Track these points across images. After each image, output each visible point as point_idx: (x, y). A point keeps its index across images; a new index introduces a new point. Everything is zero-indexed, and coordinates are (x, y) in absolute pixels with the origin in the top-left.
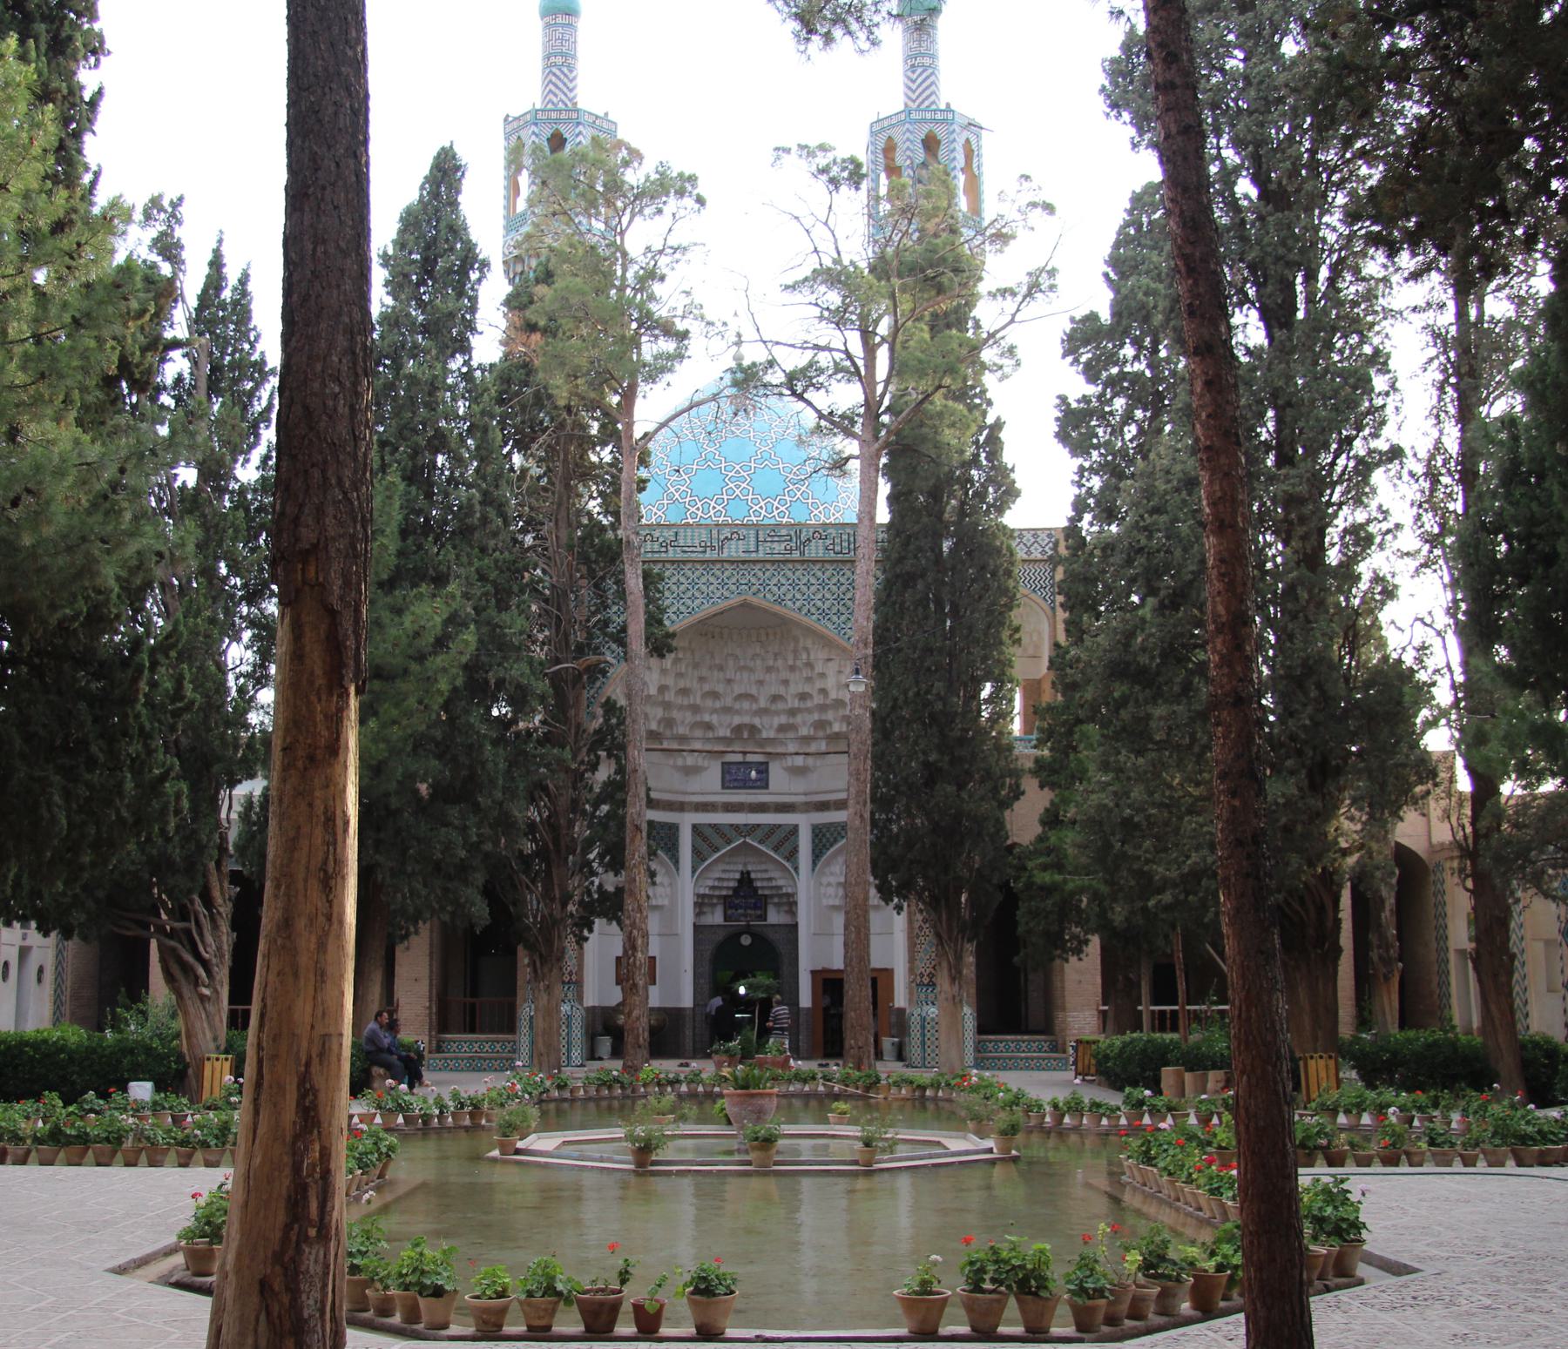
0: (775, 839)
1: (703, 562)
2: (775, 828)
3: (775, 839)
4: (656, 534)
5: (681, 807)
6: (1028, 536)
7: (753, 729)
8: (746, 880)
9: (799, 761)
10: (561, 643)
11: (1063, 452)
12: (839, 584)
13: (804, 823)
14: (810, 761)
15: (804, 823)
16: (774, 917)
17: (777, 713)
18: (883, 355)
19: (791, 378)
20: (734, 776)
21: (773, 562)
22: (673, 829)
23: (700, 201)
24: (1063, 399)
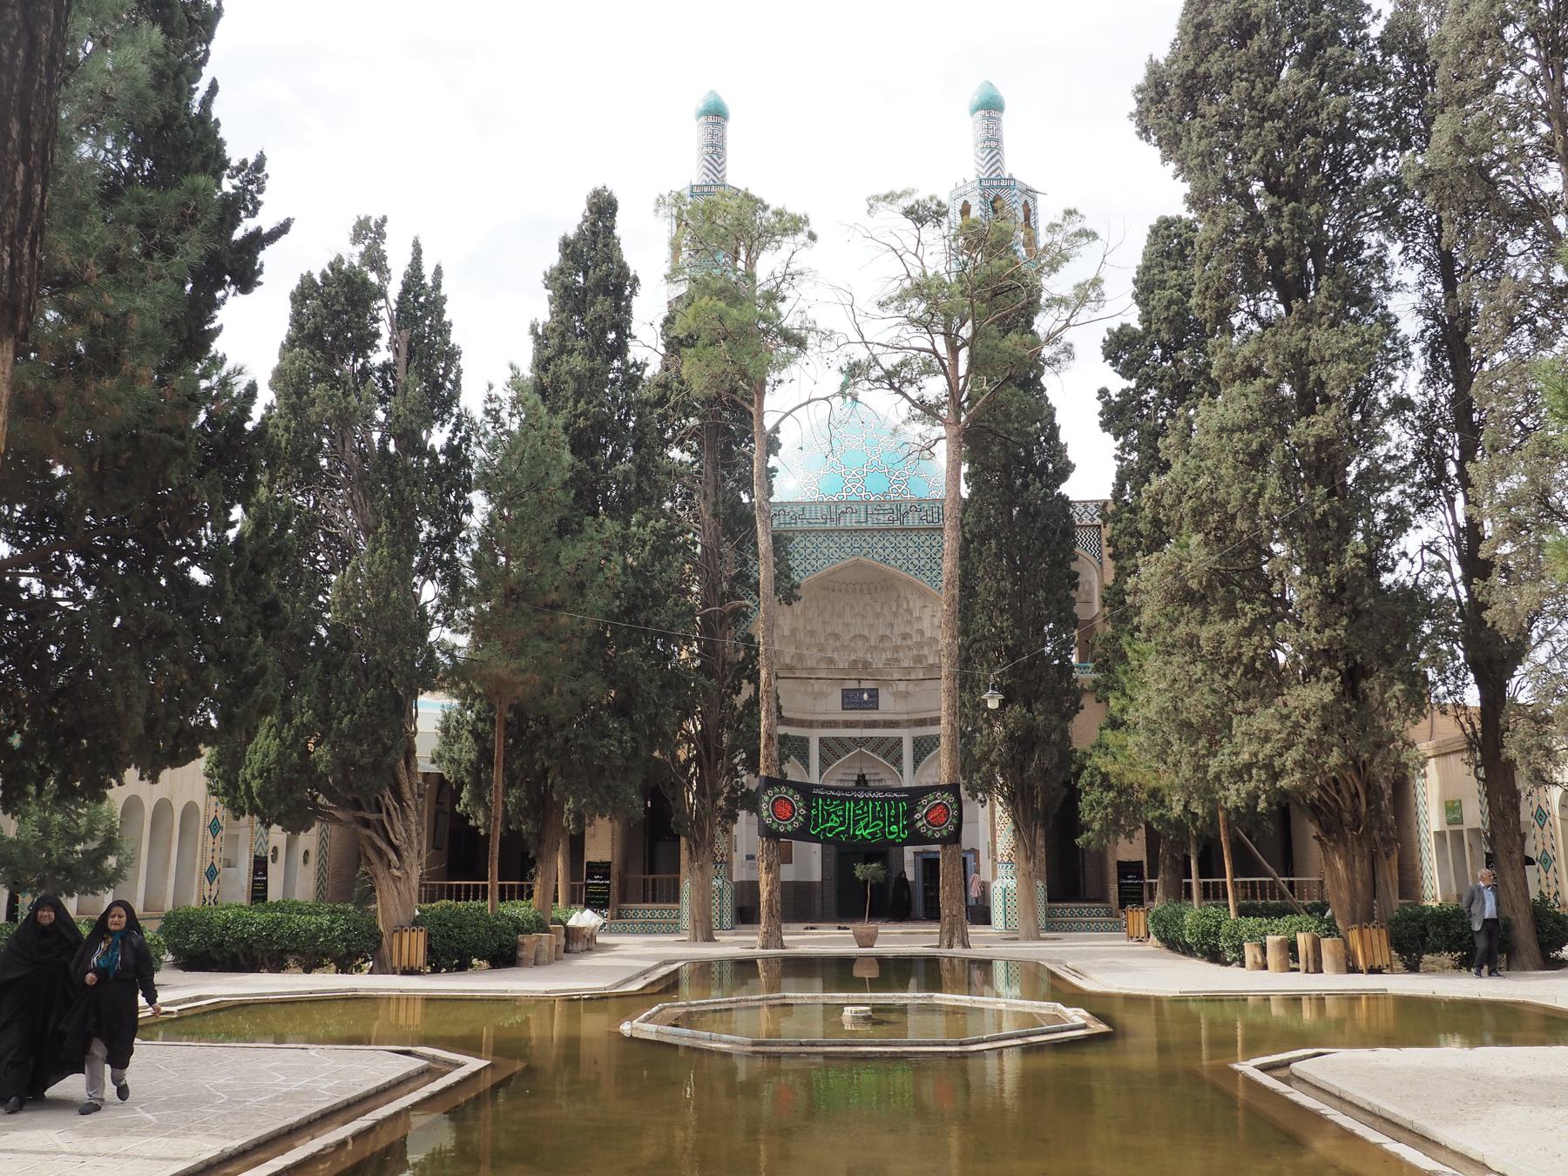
0: (883, 749)
1: (824, 531)
2: (883, 741)
3: (883, 749)
4: (788, 509)
5: (810, 724)
6: (1080, 506)
7: (866, 665)
9: (902, 686)
10: (710, 587)
11: (1109, 437)
12: (931, 547)
13: (907, 736)
14: (911, 687)
15: (907, 736)
17: (884, 650)
18: (964, 354)
19: (889, 375)
20: (851, 700)
21: (879, 530)
22: (805, 741)
23: (812, 237)
24: (1103, 393)
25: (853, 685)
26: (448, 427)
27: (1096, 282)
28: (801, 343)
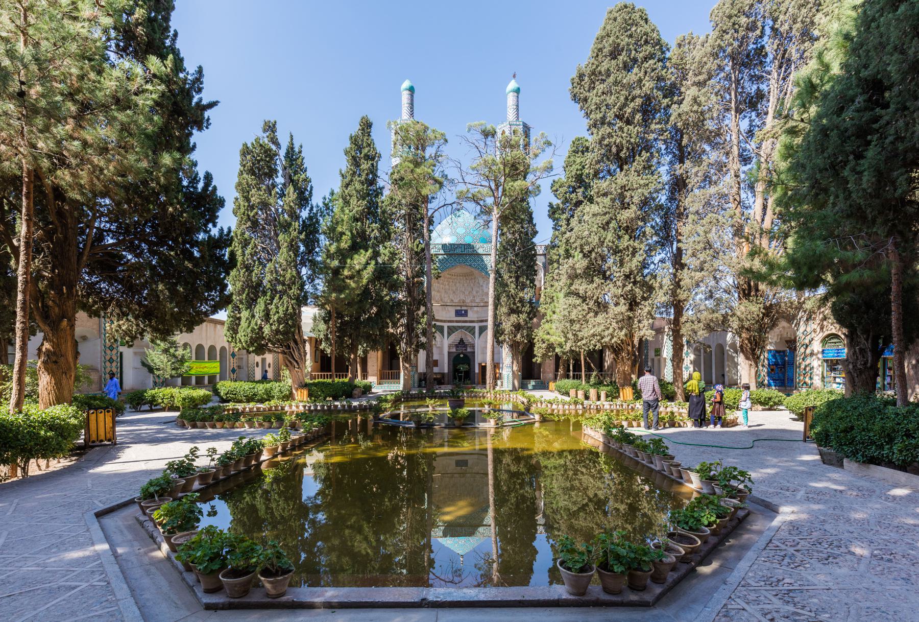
5: (445, 321)
8: (462, 340)
15: (477, 325)
16: (469, 350)
20: (458, 313)
22: (442, 327)
24: (551, 205)
25: (459, 308)
26: (308, 209)
27: (550, 162)
28: (441, 185)
